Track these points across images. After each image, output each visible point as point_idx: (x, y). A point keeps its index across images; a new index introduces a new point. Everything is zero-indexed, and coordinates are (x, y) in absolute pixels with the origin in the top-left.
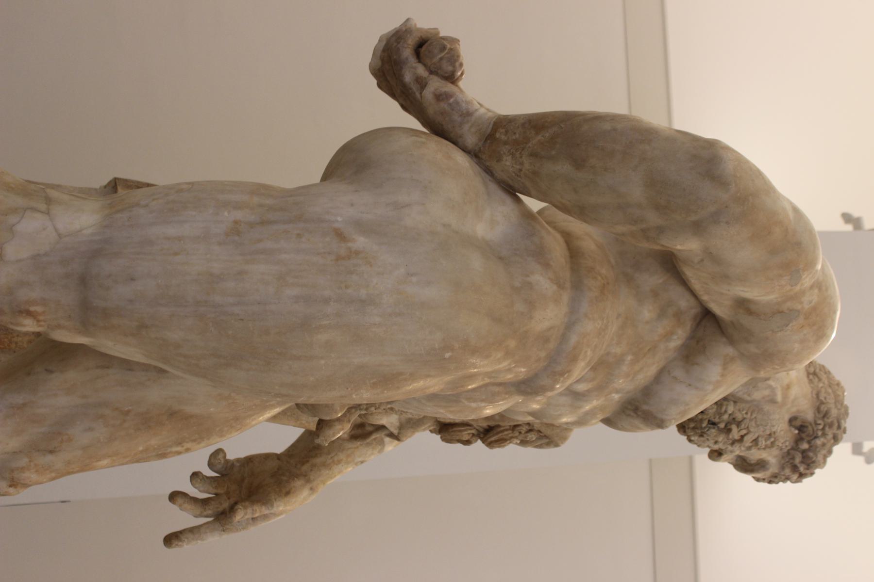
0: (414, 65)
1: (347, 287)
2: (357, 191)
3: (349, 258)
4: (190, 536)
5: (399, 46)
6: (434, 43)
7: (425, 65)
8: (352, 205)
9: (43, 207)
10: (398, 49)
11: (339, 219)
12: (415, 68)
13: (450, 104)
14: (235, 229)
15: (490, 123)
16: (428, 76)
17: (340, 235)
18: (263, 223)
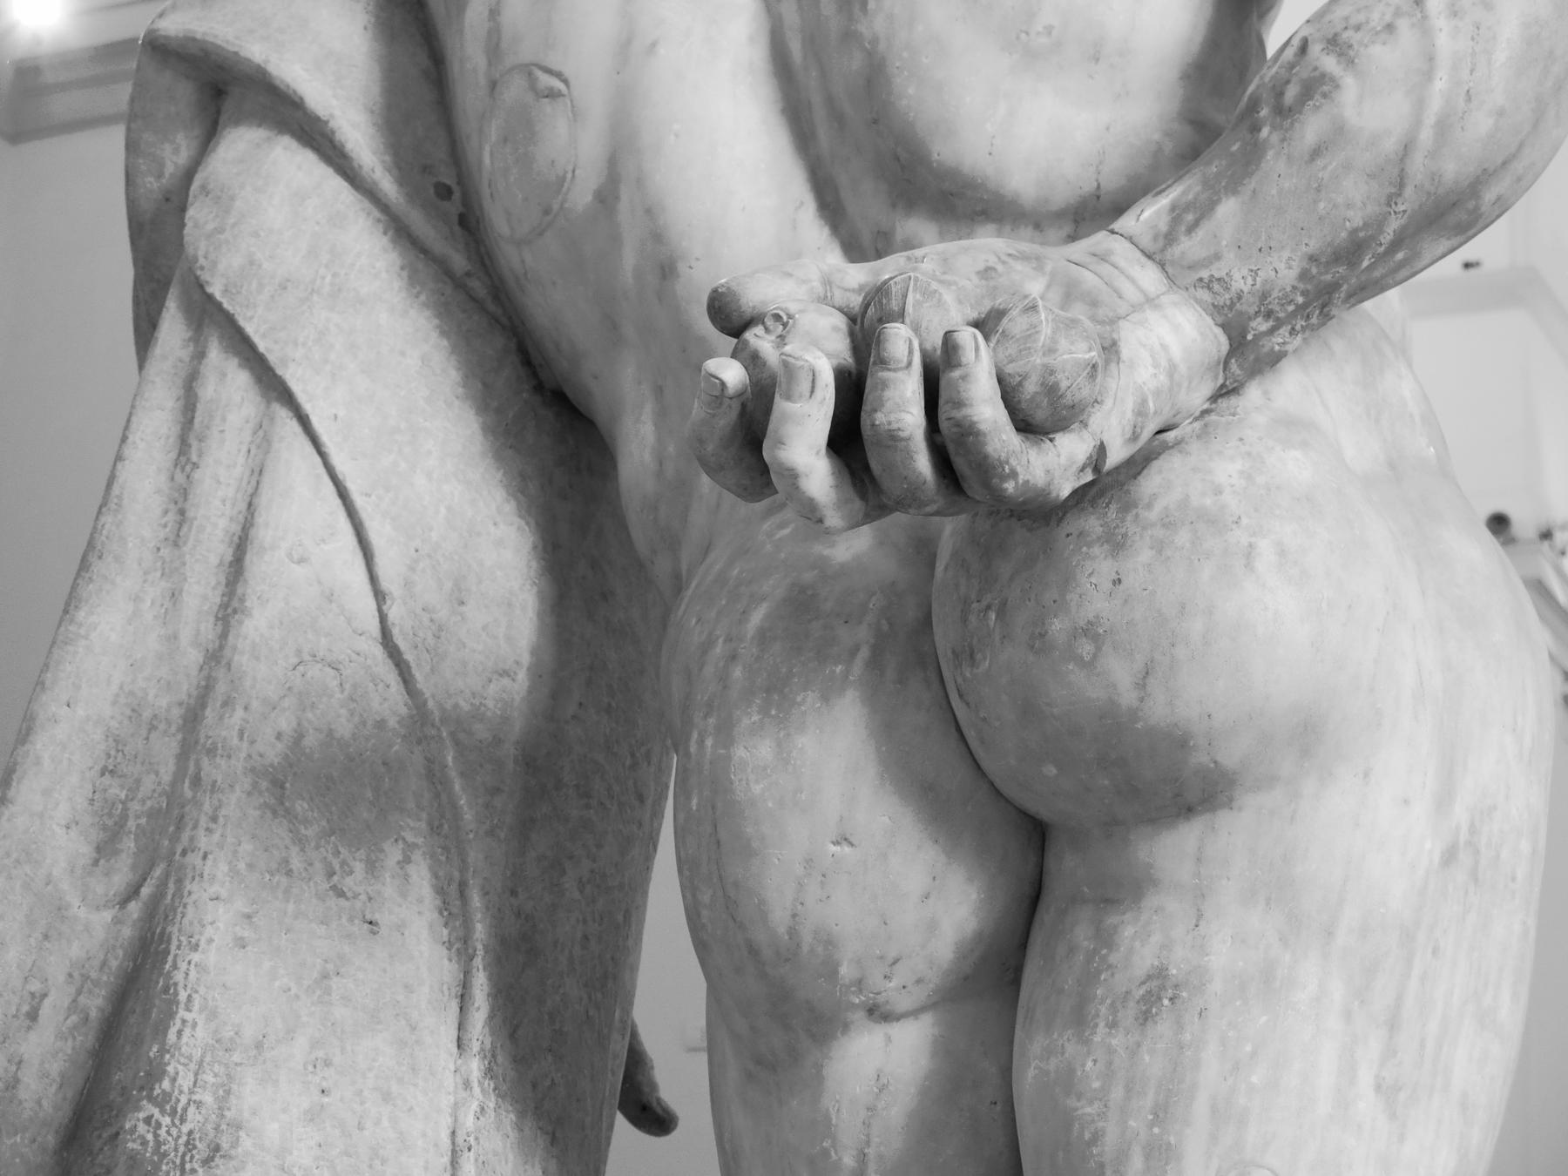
0: (1063, 460)
1: (1514, 879)
2: (1366, 775)
3: (1477, 852)
6: (1064, 384)
8: (1406, 802)
11: (1428, 845)
13: (1155, 413)
14: (1387, 1091)
15: (1216, 337)
17: (1449, 856)
18: (1393, 1024)
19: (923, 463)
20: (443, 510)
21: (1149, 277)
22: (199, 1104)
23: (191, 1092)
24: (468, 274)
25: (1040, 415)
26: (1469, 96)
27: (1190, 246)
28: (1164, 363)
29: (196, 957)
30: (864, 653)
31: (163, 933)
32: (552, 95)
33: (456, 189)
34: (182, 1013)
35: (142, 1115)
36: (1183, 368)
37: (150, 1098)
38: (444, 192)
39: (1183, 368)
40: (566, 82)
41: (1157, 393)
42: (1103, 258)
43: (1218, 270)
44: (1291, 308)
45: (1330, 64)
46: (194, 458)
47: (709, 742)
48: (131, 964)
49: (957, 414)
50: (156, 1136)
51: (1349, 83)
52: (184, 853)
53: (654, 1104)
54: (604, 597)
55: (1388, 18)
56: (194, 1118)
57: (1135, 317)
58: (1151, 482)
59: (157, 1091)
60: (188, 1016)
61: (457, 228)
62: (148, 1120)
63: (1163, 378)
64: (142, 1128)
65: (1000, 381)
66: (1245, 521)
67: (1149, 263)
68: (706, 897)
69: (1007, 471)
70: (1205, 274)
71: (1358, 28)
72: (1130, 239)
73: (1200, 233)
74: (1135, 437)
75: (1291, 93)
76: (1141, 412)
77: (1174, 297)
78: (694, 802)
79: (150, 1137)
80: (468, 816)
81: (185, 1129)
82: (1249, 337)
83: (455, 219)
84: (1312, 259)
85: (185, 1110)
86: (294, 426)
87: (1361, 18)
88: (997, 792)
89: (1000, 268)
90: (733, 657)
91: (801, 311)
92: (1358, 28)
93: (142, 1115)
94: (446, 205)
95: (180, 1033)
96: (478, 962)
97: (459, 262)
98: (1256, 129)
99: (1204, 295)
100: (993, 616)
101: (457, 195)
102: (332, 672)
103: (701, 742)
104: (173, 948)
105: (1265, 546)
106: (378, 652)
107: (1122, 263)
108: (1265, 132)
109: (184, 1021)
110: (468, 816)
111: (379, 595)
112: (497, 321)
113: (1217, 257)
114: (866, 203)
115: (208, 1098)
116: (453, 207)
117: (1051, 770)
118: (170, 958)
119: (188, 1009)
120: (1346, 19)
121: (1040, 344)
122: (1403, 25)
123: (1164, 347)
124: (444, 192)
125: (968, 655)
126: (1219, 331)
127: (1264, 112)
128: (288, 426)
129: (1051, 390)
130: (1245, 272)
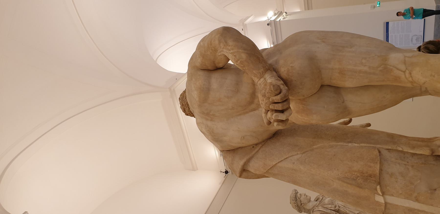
0: (283, 88)
2: (315, 52)
4: (363, 126)
5: (286, 93)
7: (280, 88)
9: (407, 59)
10: (286, 92)
11: (323, 44)
12: (283, 87)
16: (280, 85)
17: (324, 42)
19: (285, 103)
20: (287, 147)
21: (262, 80)
22: (357, 174)
23: (355, 175)
24: (262, 145)
25: (279, 91)
26: (242, 47)
28: (272, 77)
30: (303, 106)
33: (253, 146)
34: (346, 176)
36: (272, 75)
38: (253, 147)
39: (272, 75)
41: (275, 78)
42: (260, 84)
43: (261, 72)
44: (265, 64)
45: (239, 62)
47: (314, 121)
49: (279, 100)
50: (360, 179)
52: (328, 175)
53: (349, 120)
54: (295, 129)
55: (234, 56)
57: (266, 80)
58: (284, 77)
59: (355, 179)
60: (347, 175)
61: (257, 146)
62: (359, 180)
63: (273, 77)
64: (360, 181)
65: (275, 96)
66: (288, 67)
67: (261, 79)
68: (331, 121)
69: (285, 94)
70: (262, 74)
71: (235, 59)
72: (258, 81)
73: (257, 74)
74: (280, 80)
76: (277, 80)
77: (264, 76)
79: (361, 180)
80: (321, 145)
81: (360, 176)
82: (268, 68)
83: (256, 146)
84: (259, 62)
85: (357, 176)
87: (234, 59)
88: (318, 91)
89: (262, 95)
90: (304, 119)
91: (269, 116)
92: (235, 59)
94: (255, 147)
95: (349, 176)
96: (338, 143)
97: (261, 145)
98: (246, 69)
99: (264, 74)
100: (299, 93)
101: (253, 146)
102: (306, 159)
105: (291, 65)
106: (304, 154)
107: (261, 82)
108: (246, 68)
109: (347, 176)
110: (321, 145)
111: (297, 154)
112: (266, 141)
114: (253, 106)
115: (356, 173)
116: (255, 146)
117: (316, 86)
119: (346, 175)
120: (234, 60)
121: (271, 92)
122: (234, 55)
123: (270, 77)
124: (253, 147)
125: (304, 96)
126: (268, 72)
127: (244, 68)
129: (276, 90)
130: (261, 69)
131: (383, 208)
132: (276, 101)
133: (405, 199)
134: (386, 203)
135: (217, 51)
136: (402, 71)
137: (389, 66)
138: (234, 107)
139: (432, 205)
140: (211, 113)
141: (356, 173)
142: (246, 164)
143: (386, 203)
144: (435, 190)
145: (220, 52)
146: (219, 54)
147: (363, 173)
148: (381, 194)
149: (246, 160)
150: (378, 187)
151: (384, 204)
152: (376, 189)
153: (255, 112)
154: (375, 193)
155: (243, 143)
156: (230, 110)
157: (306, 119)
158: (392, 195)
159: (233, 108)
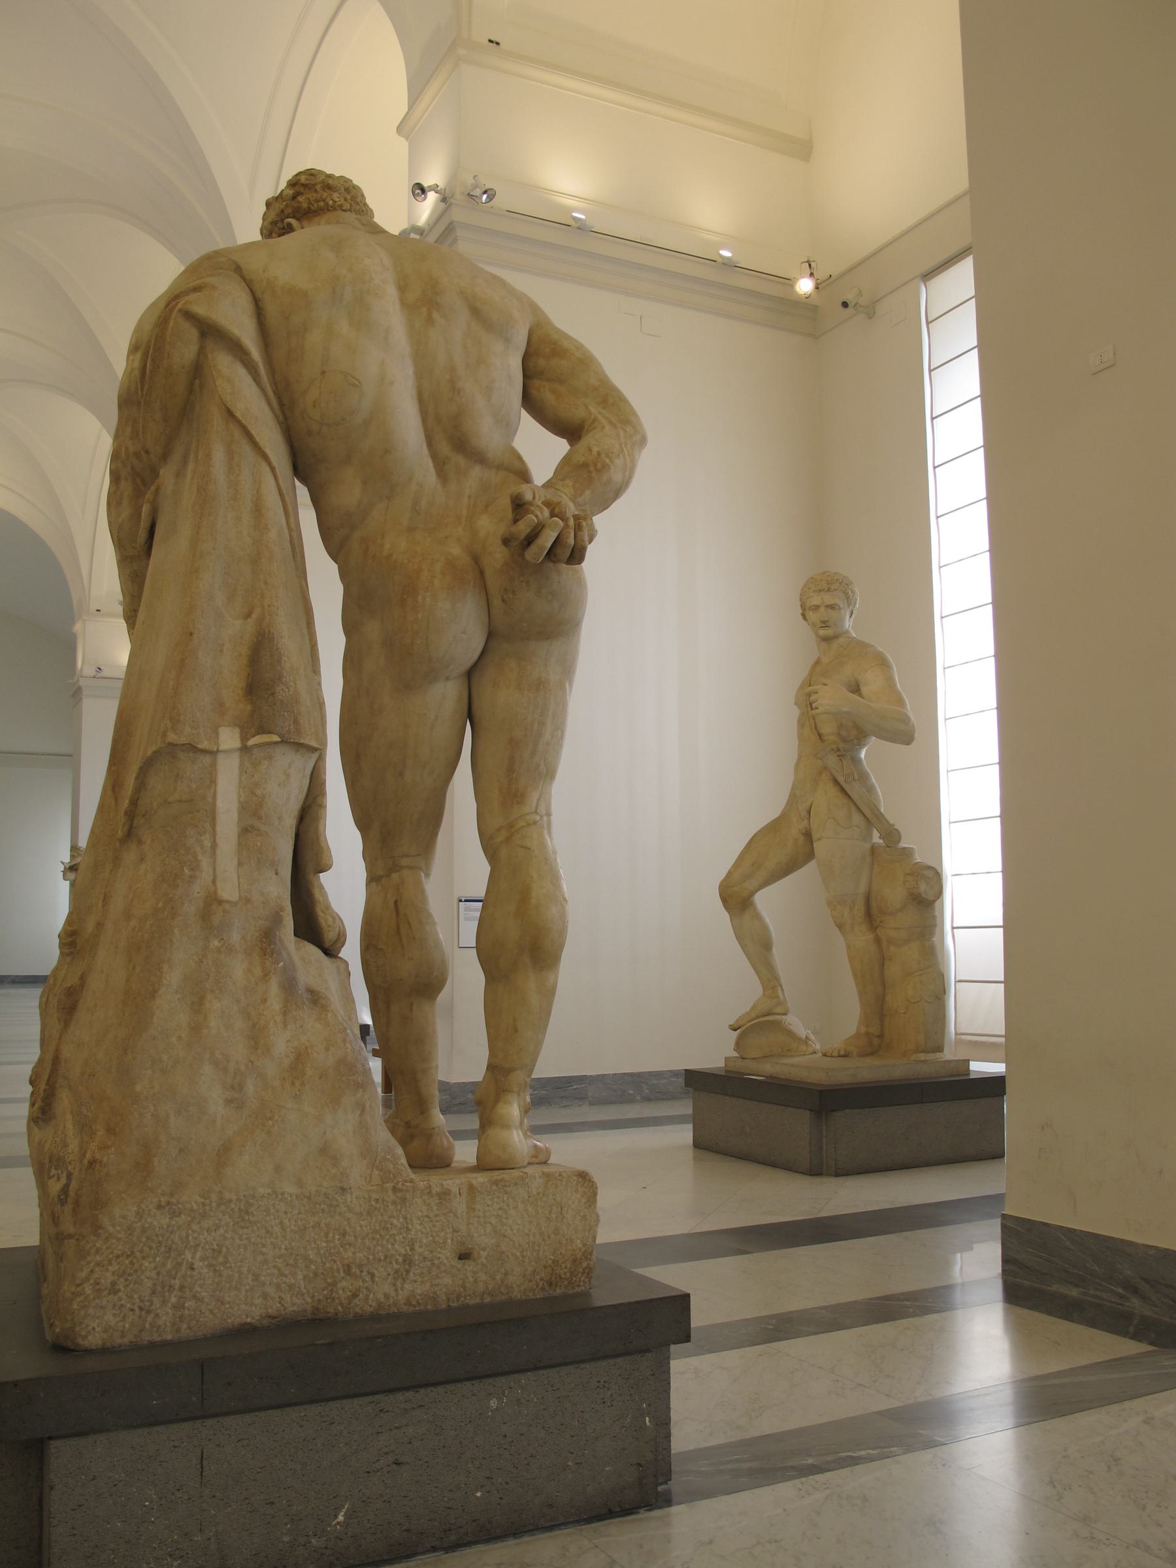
27: (580, 500)
29: (283, 640)
30: (472, 583)
31: (269, 632)
32: (354, 385)
35: (280, 688)
37: (282, 683)
40: (360, 383)
45: (607, 460)
46: (237, 472)
47: (428, 600)
48: (255, 640)
51: (612, 467)
56: (291, 689)
64: (281, 692)
70: (582, 508)
72: (564, 493)
75: (599, 466)
78: (420, 616)
86: (268, 469)
93: (280, 688)
97: (281, 418)
100: (524, 584)
103: (424, 598)
104: (276, 637)
108: (594, 475)
113: (585, 504)
114: (444, 448)
115: (293, 685)
118: (275, 640)
128: (264, 465)
131: (204, 745)
132: (579, 533)
133: (240, 802)
134: (213, 753)
135: (603, 408)
136: (537, 807)
137: (542, 783)
138: (462, 394)
139: (240, 864)
140: (436, 315)
141: (293, 685)
142: (236, 349)
143: (213, 753)
144: (277, 874)
145: (599, 413)
146: (592, 409)
147: (296, 703)
148: (251, 742)
149: (256, 360)
150: (276, 738)
151: (215, 749)
152: (262, 730)
153: (425, 445)
154: (242, 728)
155: (323, 373)
156: (448, 377)
157: (436, 582)
158: (243, 771)
159: (459, 393)
